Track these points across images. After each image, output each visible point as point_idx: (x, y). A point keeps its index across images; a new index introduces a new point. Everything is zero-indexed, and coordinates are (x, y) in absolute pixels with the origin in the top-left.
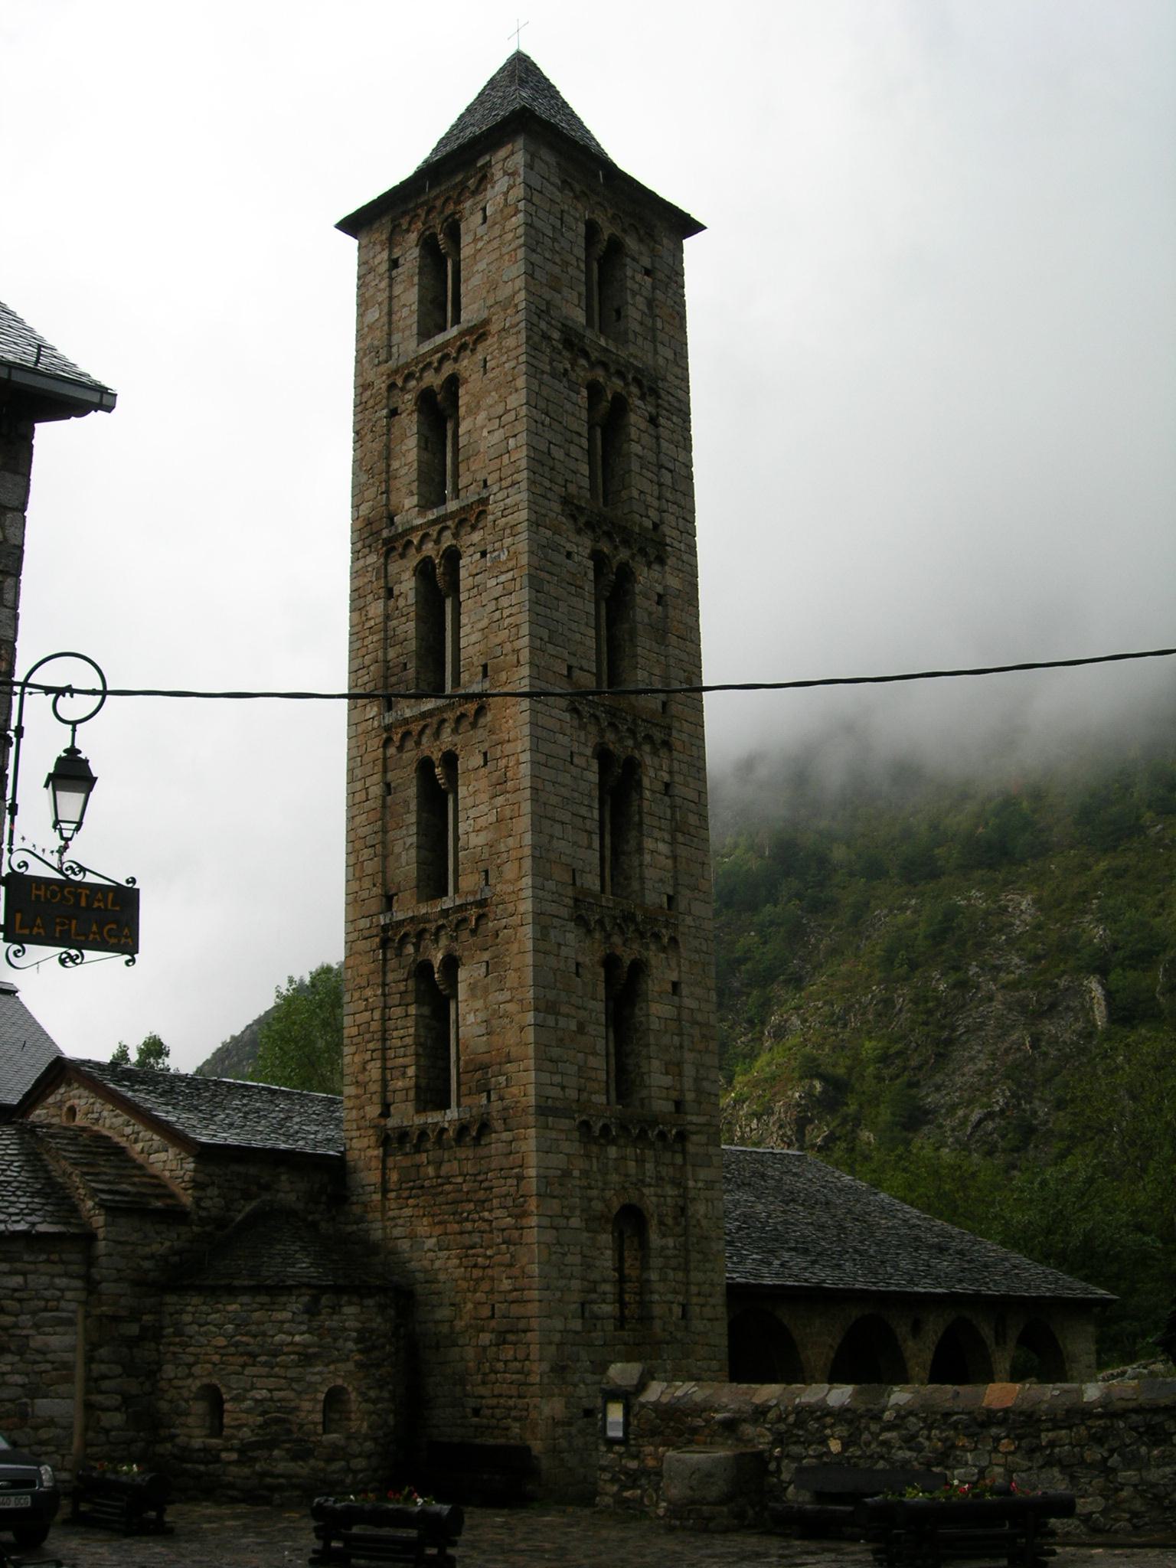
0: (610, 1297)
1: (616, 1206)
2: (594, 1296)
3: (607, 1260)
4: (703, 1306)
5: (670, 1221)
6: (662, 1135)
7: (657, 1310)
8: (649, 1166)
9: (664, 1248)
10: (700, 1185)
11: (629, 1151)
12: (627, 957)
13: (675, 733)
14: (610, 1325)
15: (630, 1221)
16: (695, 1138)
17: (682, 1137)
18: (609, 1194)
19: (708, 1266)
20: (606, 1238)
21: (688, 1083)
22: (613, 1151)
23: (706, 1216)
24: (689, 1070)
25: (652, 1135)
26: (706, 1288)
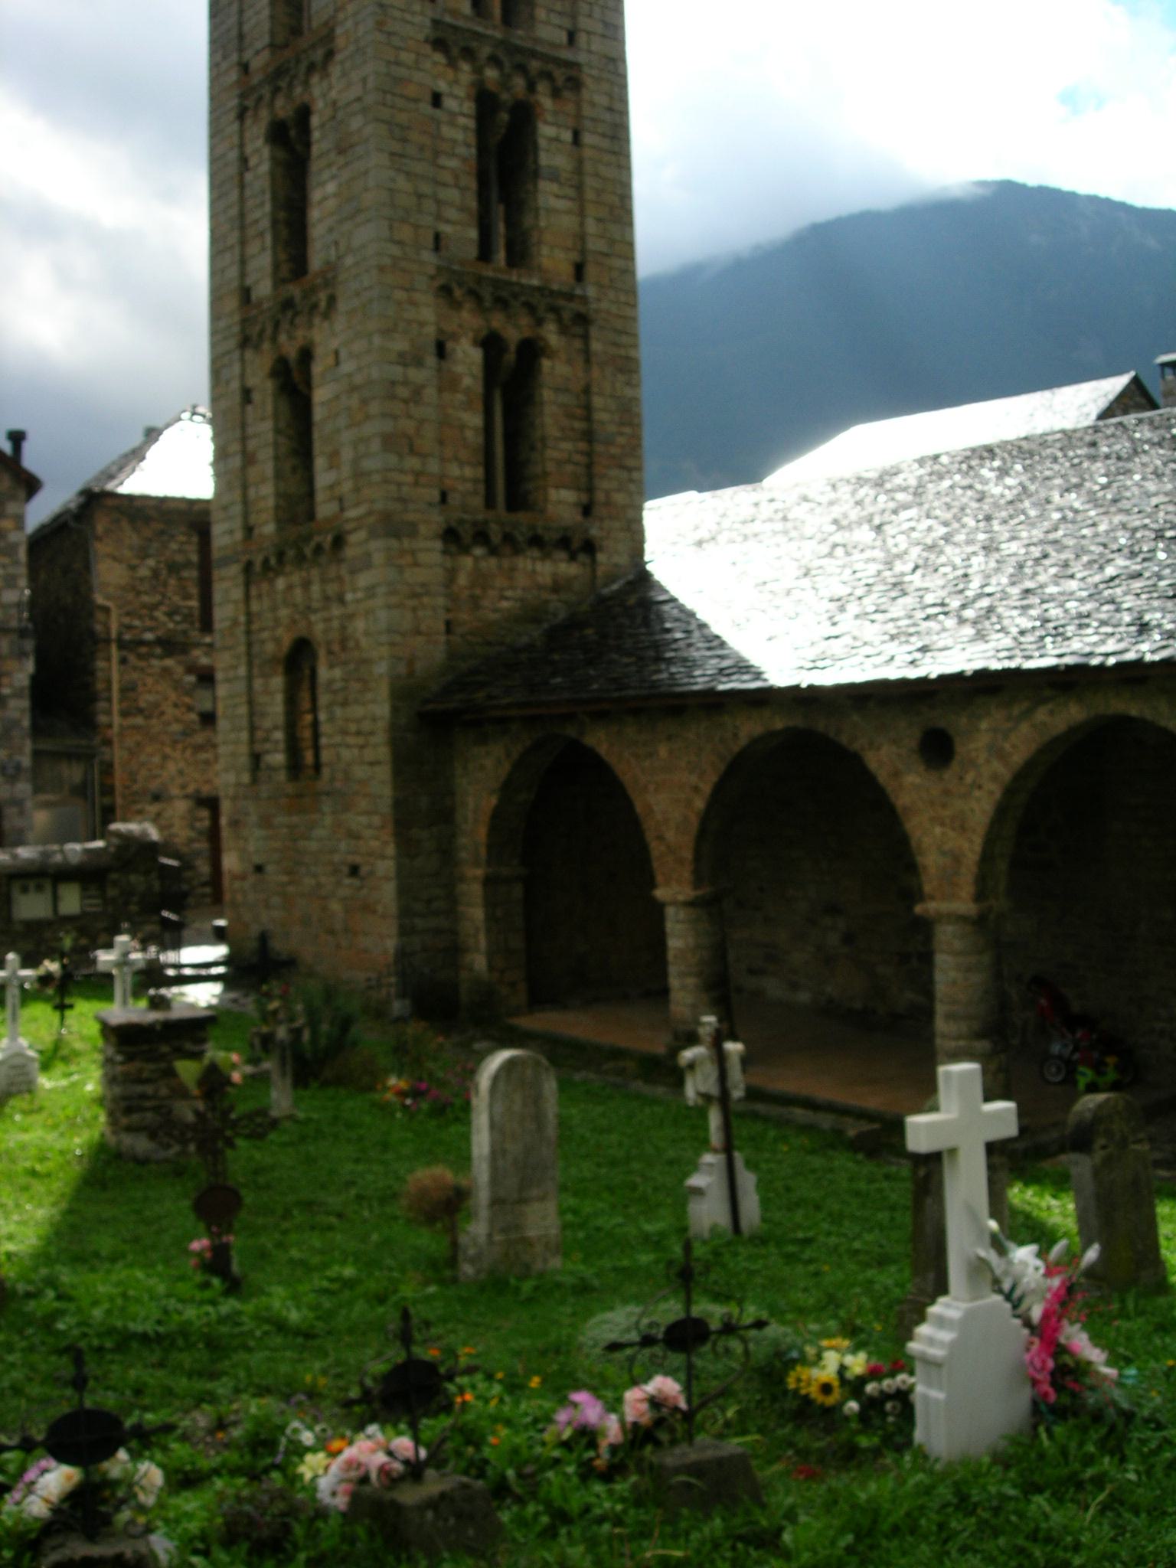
0: (282, 746)
1: (287, 641)
2: (268, 746)
3: (275, 708)
4: (362, 747)
5: (336, 648)
6: (318, 550)
7: (326, 756)
8: (315, 589)
9: (331, 682)
10: (360, 595)
11: (296, 578)
12: (291, 351)
13: (339, 31)
14: (282, 776)
15: (299, 659)
16: (353, 538)
17: (339, 542)
18: (280, 631)
19: (369, 696)
20: (278, 682)
21: (346, 470)
22: (281, 583)
23: (367, 633)
24: (347, 454)
25: (308, 551)
26: (366, 726)
